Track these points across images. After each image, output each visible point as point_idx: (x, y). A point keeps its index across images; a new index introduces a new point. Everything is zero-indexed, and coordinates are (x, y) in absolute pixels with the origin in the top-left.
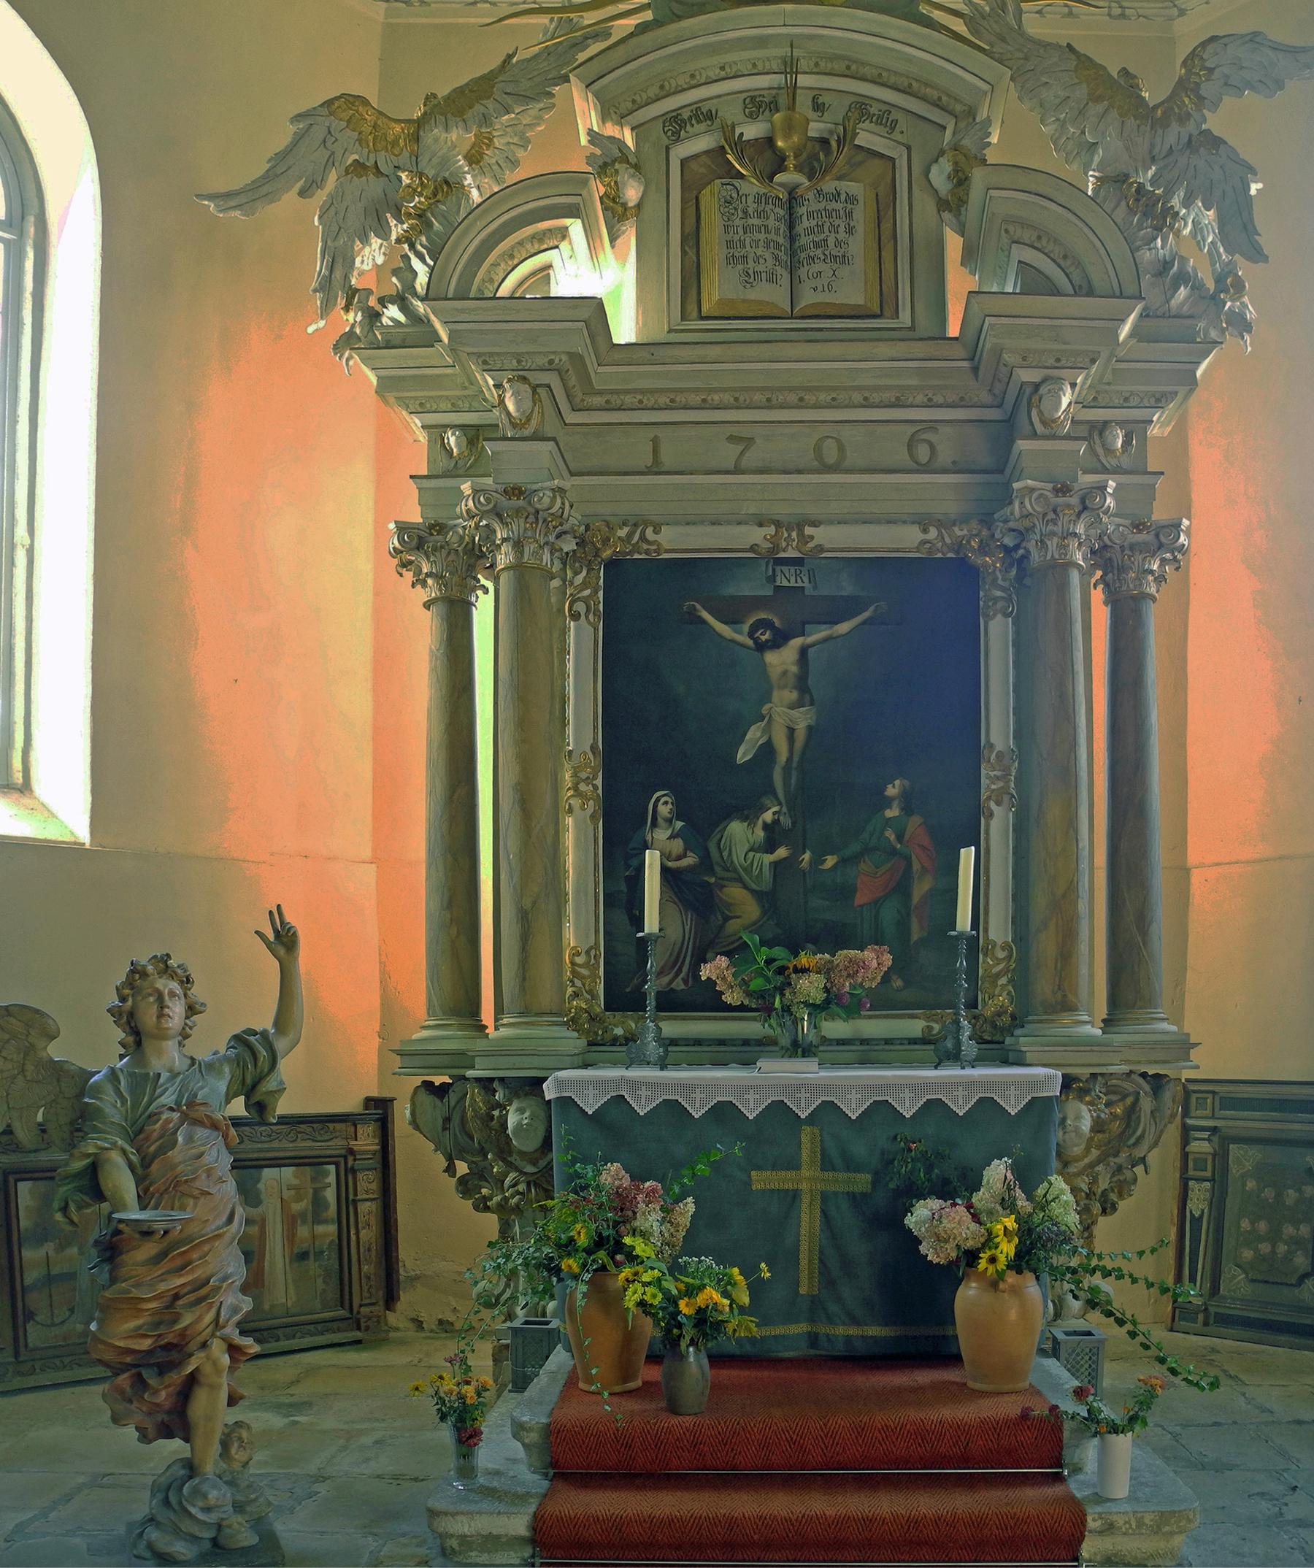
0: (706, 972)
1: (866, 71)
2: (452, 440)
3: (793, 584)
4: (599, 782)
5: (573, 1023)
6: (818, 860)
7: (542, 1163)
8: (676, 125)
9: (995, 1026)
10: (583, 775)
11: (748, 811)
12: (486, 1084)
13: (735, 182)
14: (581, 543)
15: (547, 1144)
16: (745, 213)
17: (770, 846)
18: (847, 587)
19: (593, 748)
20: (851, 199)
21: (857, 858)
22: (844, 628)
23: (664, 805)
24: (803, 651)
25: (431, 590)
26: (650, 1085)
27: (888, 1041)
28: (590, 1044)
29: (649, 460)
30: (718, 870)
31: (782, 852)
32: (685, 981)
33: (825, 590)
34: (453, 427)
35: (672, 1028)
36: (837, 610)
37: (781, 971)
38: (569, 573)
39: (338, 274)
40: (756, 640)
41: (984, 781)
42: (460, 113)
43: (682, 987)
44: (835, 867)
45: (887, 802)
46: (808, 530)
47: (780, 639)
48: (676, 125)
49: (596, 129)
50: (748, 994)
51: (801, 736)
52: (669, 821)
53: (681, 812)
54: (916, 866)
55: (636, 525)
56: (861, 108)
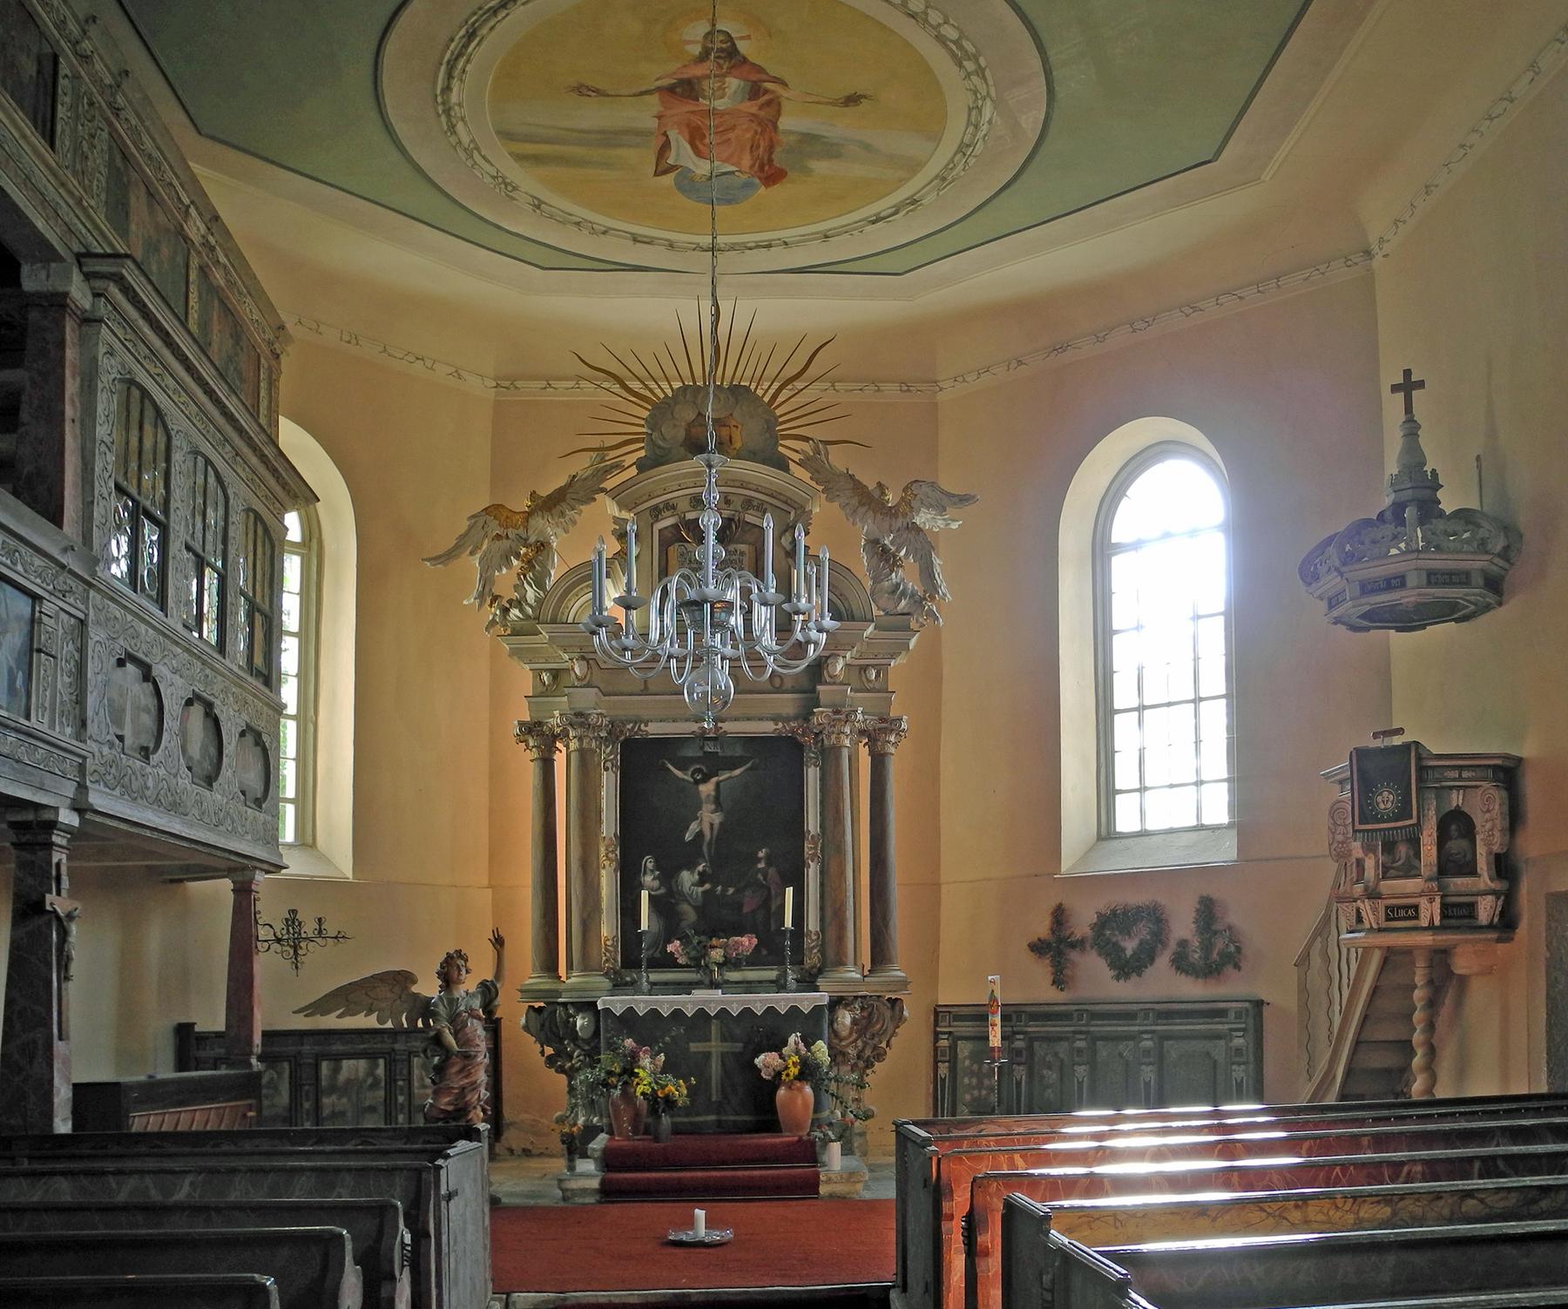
0: (670, 948)
1: (751, 486)
2: (545, 677)
3: (712, 750)
4: (618, 852)
5: (606, 975)
6: (724, 890)
7: (592, 1044)
8: (656, 512)
9: (810, 974)
10: (610, 849)
11: (691, 866)
12: (565, 1005)
13: (685, 544)
14: (610, 733)
15: (596, 1033)
16: (690, 561)
17: (701, 883)
18: (738, 751)
19: (615, 834)
20: (742, 553)
21: (746, 887)
22: (737, 772)
23: (649, 862)
24: (718, 784)
25: (535, 754)
26: (646, 1002)
27: (760, 982)
28: (614, 986)
29: (642, 687)
30: (677, 897)
31: (707, 886)
32: (660, 952)
33: (729, 753)
34: (546, 670)
35: (654, 977)
36: (732, 764)
37: (705, 946)
38: (603, 747)
39: (487, 590)
40: (695, 779)
41: (806, 849)
42: (549, 510)
43: (659, 955)
44: (733, 894)
45: (759, 860)
46: (720, 725)
47: (705, 780)
48: (656, 512)
49: (617, 515)
50: (690, 959)
51: (716, 827)
52: (652, 871)
53: (658, 866)
54: (773, 892)
55: (636, 723)
56: (748, 503)
